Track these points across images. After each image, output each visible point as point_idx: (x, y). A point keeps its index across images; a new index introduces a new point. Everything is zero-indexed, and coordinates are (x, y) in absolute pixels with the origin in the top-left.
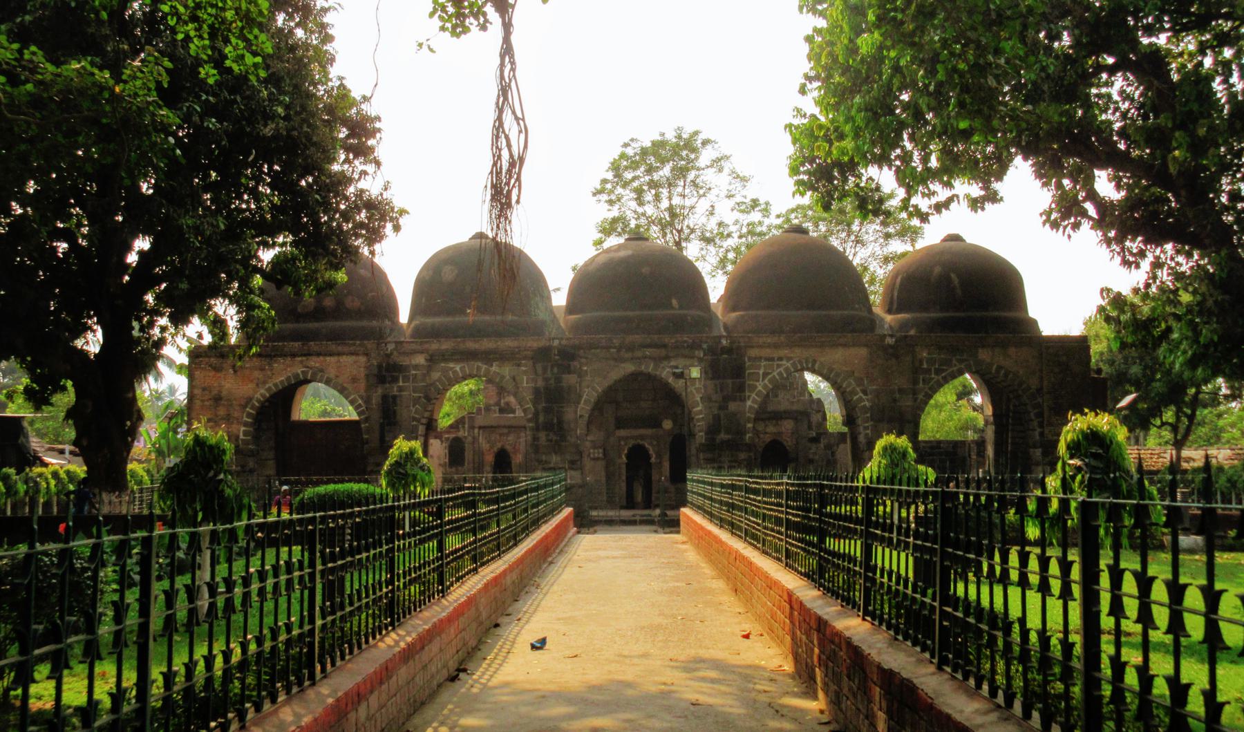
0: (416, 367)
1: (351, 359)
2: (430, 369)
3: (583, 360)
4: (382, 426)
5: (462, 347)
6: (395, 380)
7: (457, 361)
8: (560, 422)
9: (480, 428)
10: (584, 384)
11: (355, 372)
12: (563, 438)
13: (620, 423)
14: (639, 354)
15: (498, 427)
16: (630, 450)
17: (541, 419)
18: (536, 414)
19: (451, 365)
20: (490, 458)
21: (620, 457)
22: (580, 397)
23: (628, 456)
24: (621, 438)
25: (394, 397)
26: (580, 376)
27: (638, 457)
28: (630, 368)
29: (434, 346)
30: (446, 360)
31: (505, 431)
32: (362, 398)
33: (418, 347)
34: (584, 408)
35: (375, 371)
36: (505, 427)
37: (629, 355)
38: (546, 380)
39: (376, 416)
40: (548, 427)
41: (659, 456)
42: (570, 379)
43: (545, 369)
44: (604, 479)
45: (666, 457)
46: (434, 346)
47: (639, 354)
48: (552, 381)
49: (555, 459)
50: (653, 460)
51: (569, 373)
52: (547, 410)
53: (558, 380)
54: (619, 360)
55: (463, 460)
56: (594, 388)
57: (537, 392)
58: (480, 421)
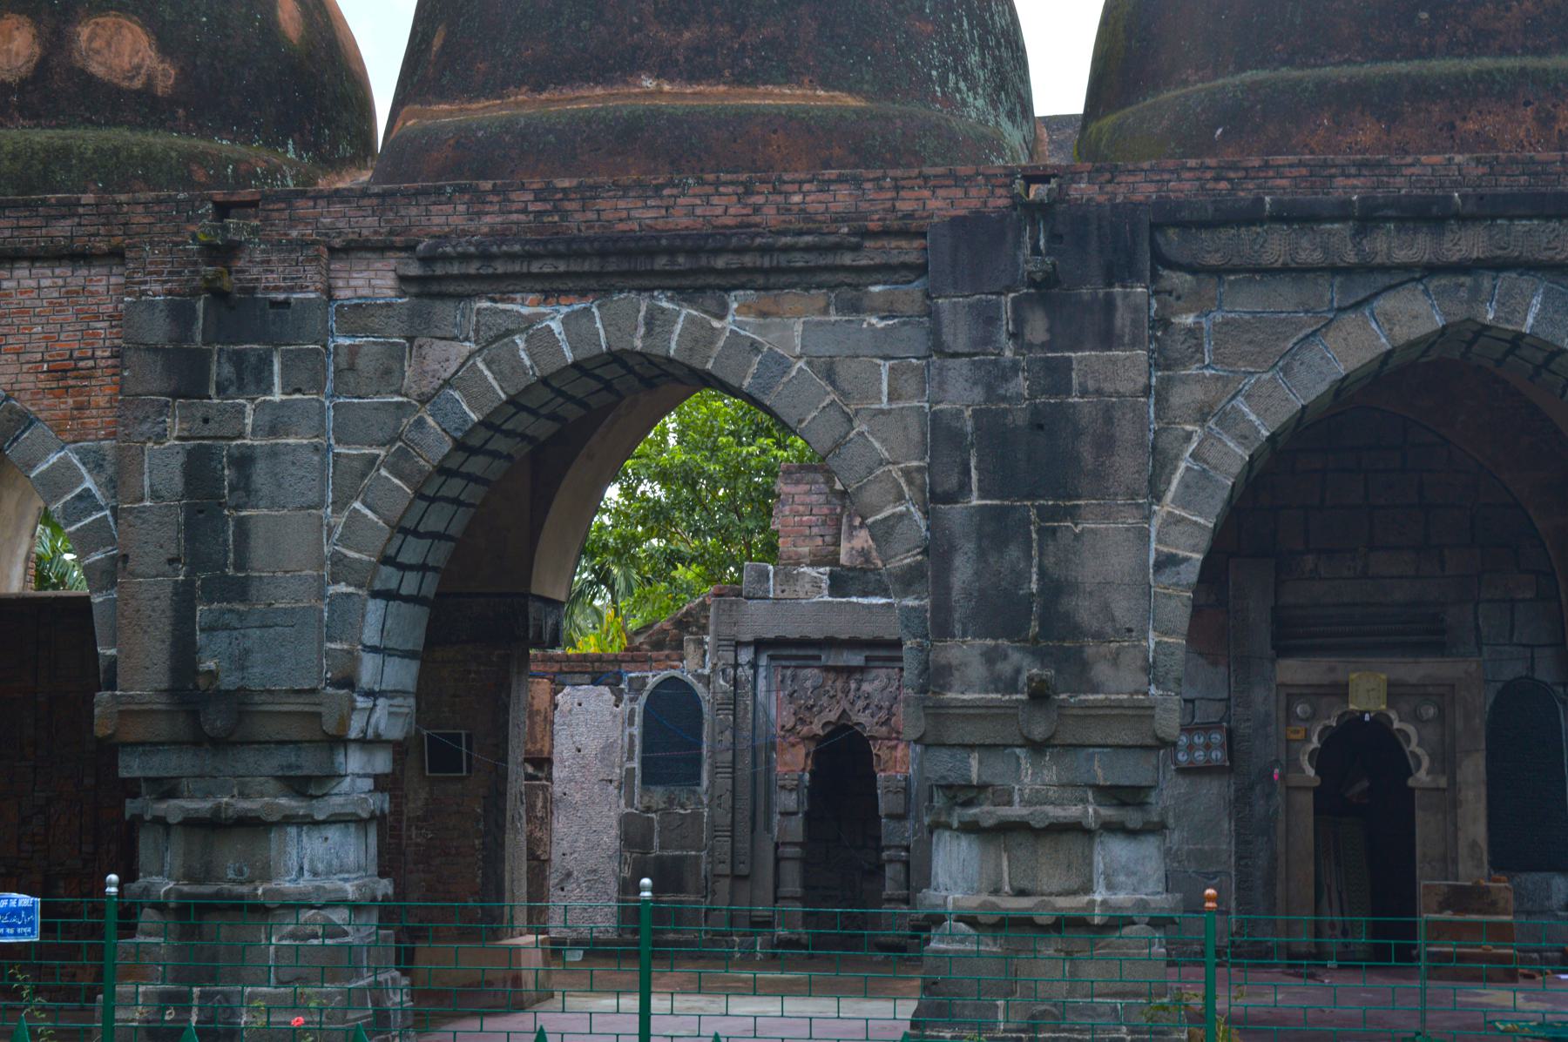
0: (358, 315)
1: (49, 279)
2: (418, 329)
3: (1178, 280)
4: (184, 601)
5: (579, 220)
6: (253, 376)
7: (551, 289)
8: (1055, 589)
9: (760, 645)
10: (1180, 397)
11: (69, 340)
12: (1077, 668)
13: (1290, 639)
14: (1468, 243)
15: (831, 643)
16: (1331, 739)
17: (963, 572)
18: (938, 551)
19: (524, 307)
20: (793, 763)
21: (1292, 764)
22: (1161, 462)
23: (1319, 759)
24: (1292, 694)
25: (243, 461)
26: (1163, 361)
27: (1363, 772)
28: (1415, 315)
29: (448, 217)
30: (503, 285)
31: (856, 659)
32: (96, 463)
33: (369, 225)
34: (1183, 523)
35: (158, 330)
36: (854, 644)
37: (1417, 248)
38: (994, 376)
39: (156, 540)
40: (1002, 614)
41: (1446, 761)
42: (1122, 369)
43: (987, 318)
44: (1227, 846)
45: (1473, 769)
46: (448, 217)
47: (1468, 243)
48: (1021, 384)
49: (1032, 787)
50: (1422, 777)
51: (1108, 339)
52: (997, 530)
53: (1056, 376)
54: (1368, 279)
55: (697, 762)
56: (1228, 419)
57: (941, 434)
58: (758, 620)
